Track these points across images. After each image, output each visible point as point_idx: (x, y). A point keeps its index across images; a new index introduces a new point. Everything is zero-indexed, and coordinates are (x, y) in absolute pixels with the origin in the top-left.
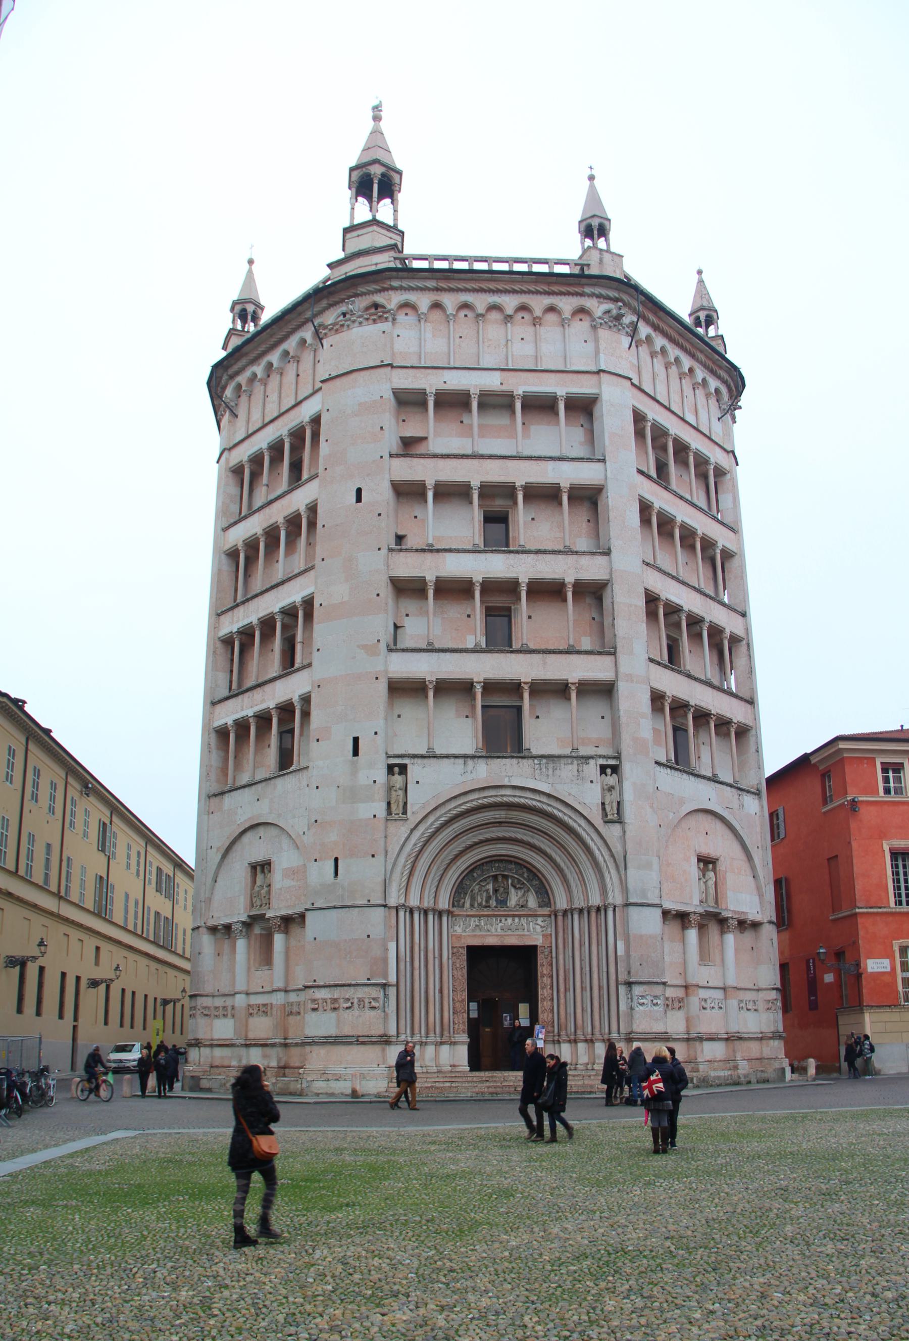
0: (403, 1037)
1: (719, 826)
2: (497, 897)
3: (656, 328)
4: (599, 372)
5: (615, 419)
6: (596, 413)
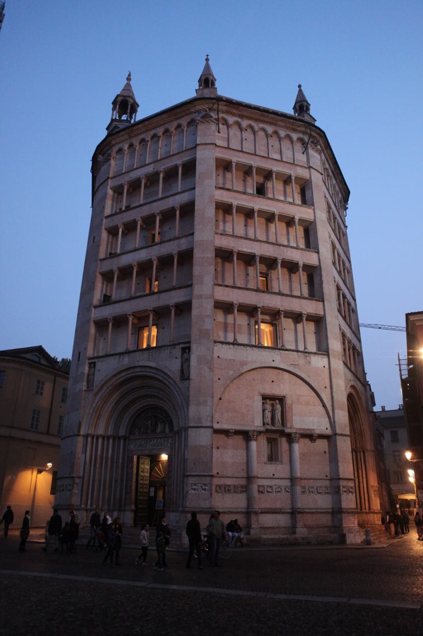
0: (83, 506)
1: (286, 375)
3: (242, 117)
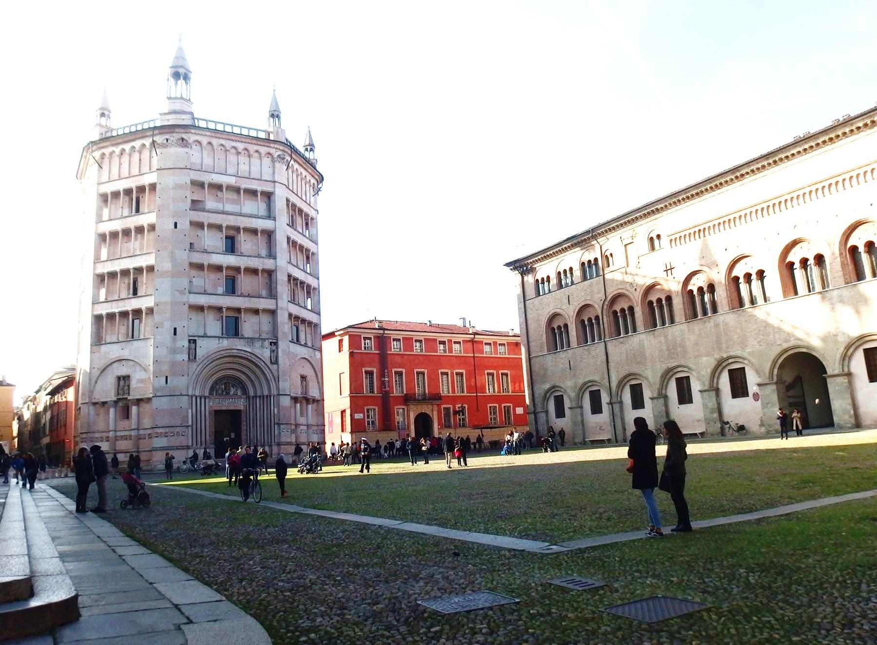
3: (295, 161)
4: (274, 182)
5: (280, 204)
6: (272, 198)
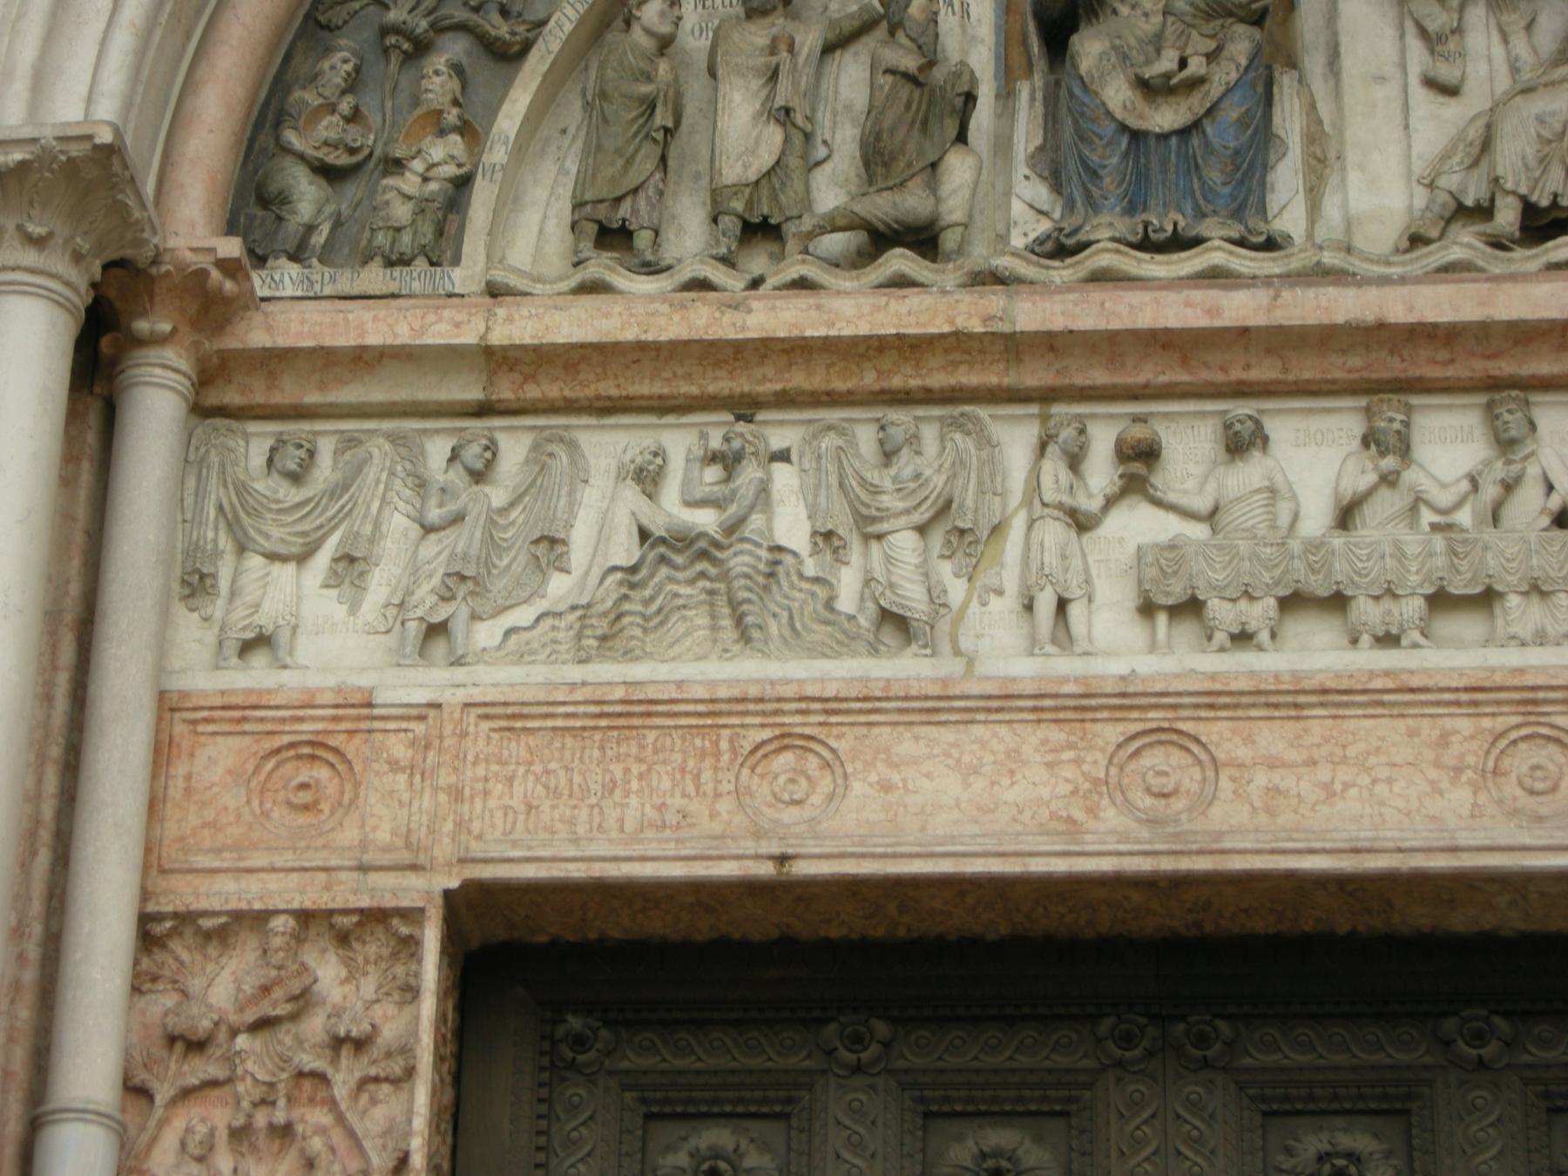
2: (1066, 106)
